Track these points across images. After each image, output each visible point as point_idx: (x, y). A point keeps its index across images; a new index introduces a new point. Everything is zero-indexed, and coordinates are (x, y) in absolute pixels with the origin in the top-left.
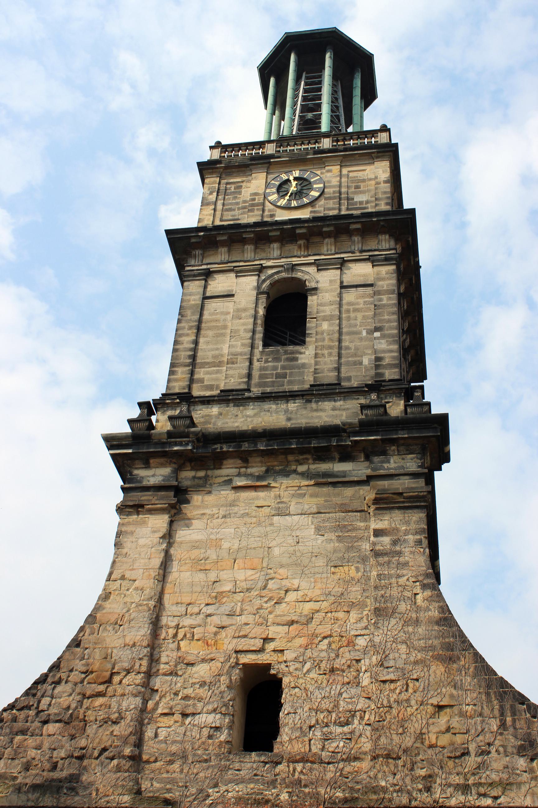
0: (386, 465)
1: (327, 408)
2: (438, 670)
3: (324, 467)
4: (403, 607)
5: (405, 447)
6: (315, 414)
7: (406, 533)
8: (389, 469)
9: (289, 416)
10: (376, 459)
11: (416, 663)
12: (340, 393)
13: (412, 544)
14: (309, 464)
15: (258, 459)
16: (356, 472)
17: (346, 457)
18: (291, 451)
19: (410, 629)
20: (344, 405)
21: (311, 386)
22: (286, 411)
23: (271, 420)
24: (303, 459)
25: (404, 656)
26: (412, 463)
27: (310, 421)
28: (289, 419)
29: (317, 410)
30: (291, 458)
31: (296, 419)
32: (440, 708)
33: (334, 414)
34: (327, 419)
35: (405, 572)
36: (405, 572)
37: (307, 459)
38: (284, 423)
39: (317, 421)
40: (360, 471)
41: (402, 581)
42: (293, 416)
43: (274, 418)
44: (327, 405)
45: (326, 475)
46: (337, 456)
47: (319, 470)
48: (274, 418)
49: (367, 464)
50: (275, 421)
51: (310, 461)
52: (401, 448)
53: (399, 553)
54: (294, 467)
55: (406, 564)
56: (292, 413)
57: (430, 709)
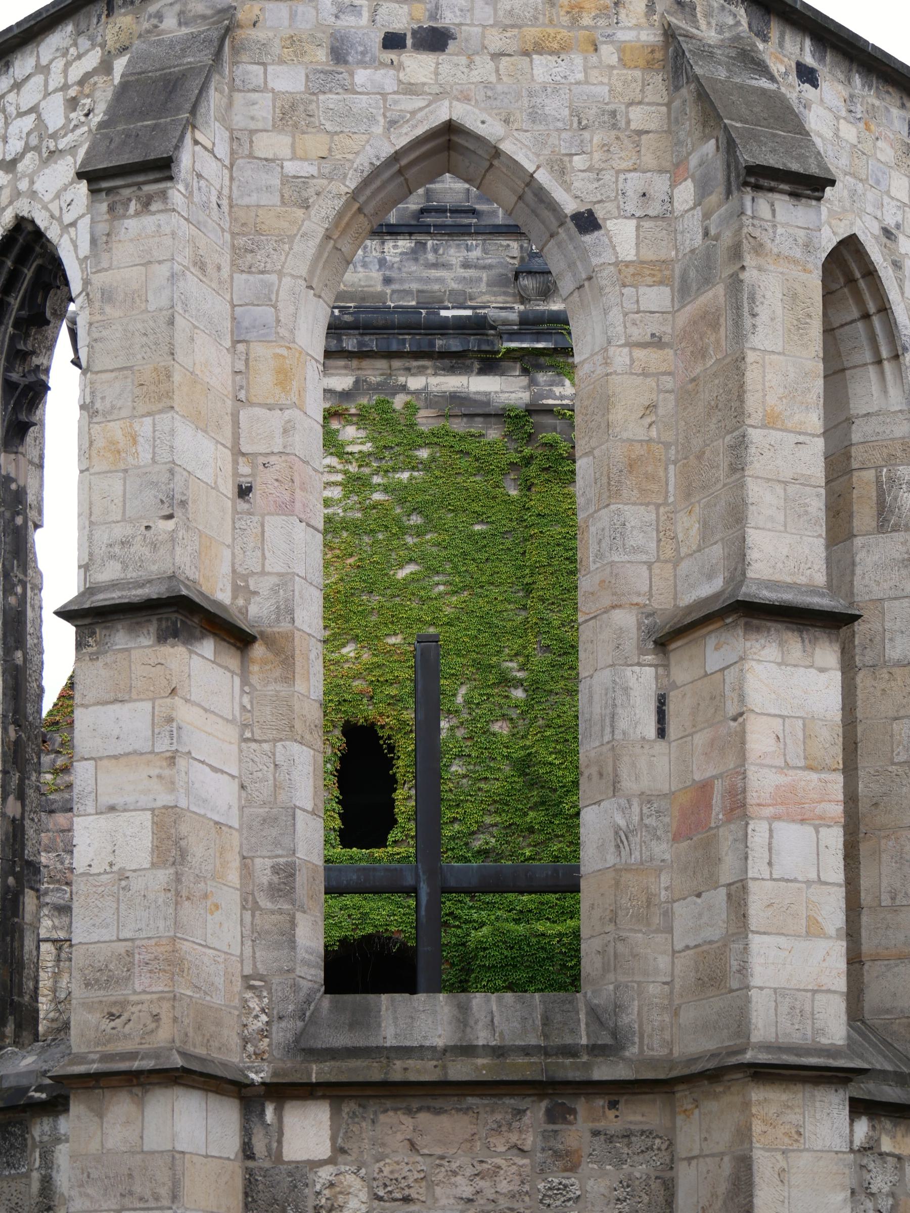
0: (557, 390)
1: (454, 261)
3: (453, 383)
6: (434, 273)
8: (562, 397)
9: (387, 273)
10: (542, 377)
12: (477, 233)
14: (427, 375)
15: (342, 363)
16: (507, 395)
17: (490, 364)
18: (399, 355)
20: (483, 259)
21: (423, 211)
22: (382, 262)
23: (356, 280)
24: (419, 367)
27: (425, 288)
28: (387, 281)
29: (435, 266)
30: (397, 363)
31: (402, 281)
33: (466, 275)
34: (454, 286)
37: (425, 368)
38: (379, 288)
39: (436, 287)
40: (513, 395)
42: (394, 274)
43: (361, 275)
44: (455, 253)
45: (455, 398)
46: (477, 365)
47: (444, 388)
48: (361, 275)
49: (524, 380)
50: (362, 283)
51: (429, 371)
54: (402, 380)
56: (391, 267)
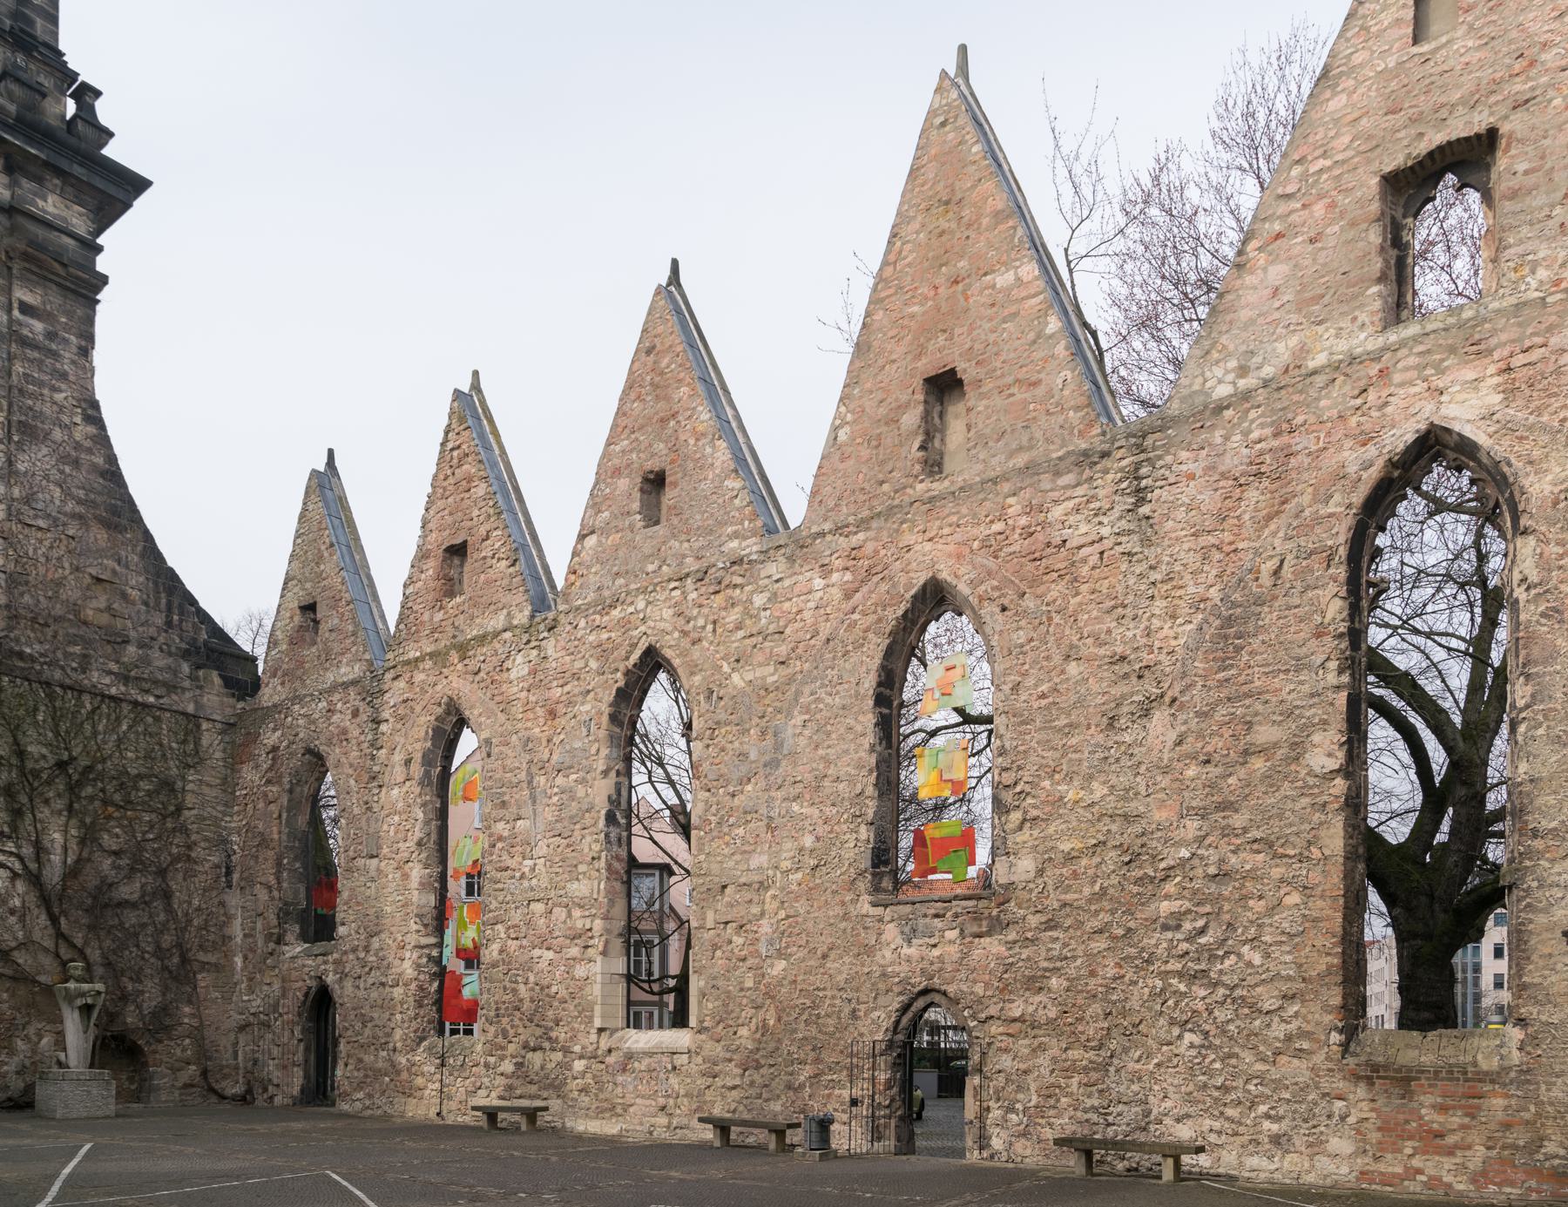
2: (99, 536)
4: (58, 434)
5: (76, 190)
7: (67, 329)
11: (74, 516)
13: (75, 350)
19: (67, 469)
25: (57, 502)
26: (79, 223)
32: (99, 580)
35: (63, 386)
36: (63, 386)
41: (59, 397)
52: (69, 189)
53: (55, 355)
55: (64, 376)
57: (88, 580)
